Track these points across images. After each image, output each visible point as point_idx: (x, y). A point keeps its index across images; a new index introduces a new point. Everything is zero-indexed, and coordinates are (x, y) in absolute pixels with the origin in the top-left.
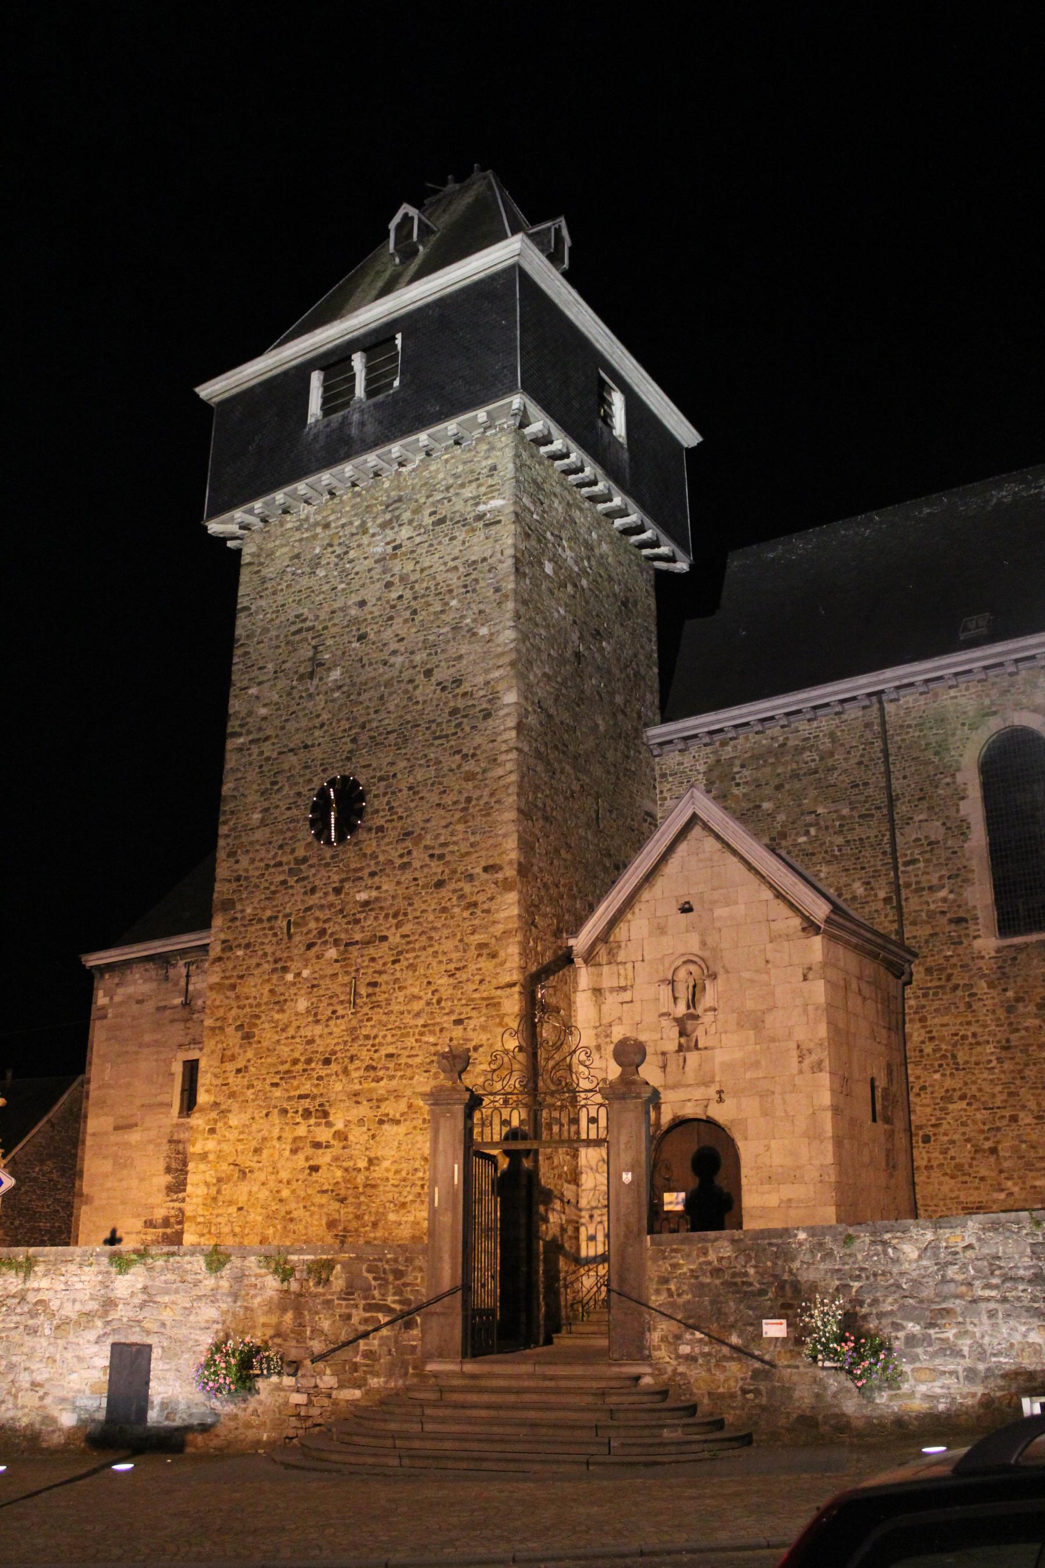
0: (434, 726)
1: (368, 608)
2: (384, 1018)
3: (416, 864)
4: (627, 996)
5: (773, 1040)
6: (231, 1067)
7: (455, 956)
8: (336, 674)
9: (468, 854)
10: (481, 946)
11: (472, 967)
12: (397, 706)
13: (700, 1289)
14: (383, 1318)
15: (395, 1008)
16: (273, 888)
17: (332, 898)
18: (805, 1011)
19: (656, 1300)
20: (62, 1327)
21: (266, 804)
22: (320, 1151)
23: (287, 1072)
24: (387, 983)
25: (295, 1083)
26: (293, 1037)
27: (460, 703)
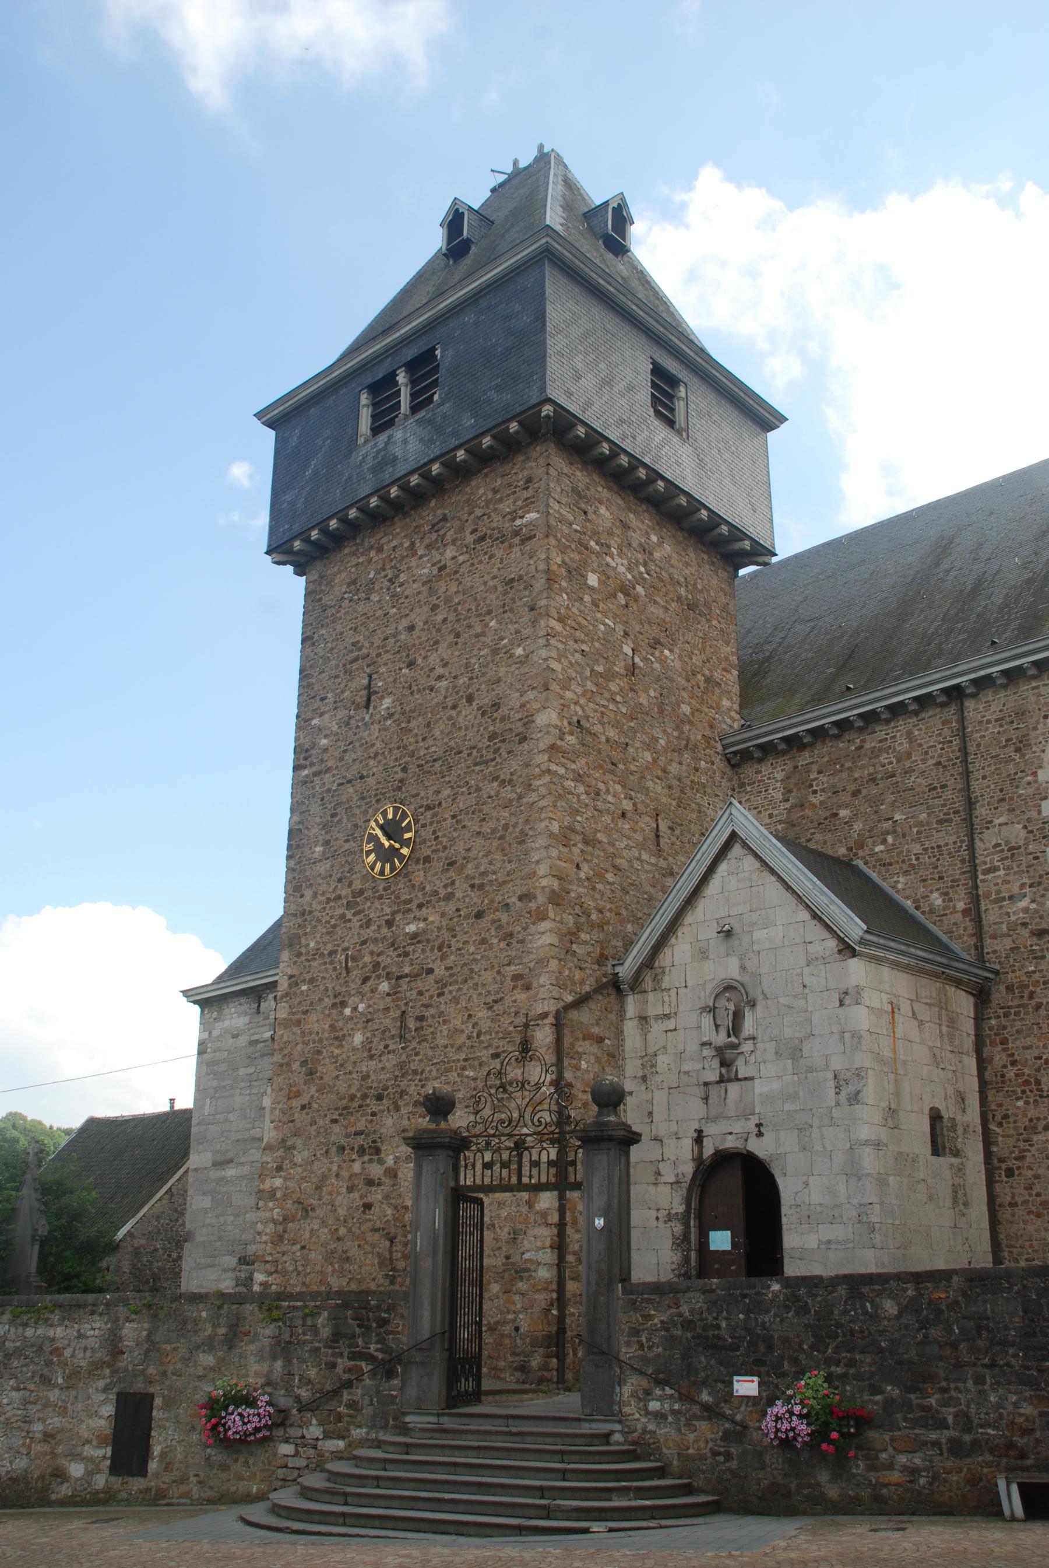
0: (474, 752)
1: (416, 633)
2: (430, 1053)
3: (459, 894)
4: (670, 1024)
5: (810, 1070)
6: (296, 1103)
7: (492, 988)
8: (387, 702)
9: (505, 882)
10: (517, 977)
11: (508, 1000)
12: (442, 732)
13: (671, 1341)
14: (365, 1366)
15: (440, 1042)
16: (333, 922)
17: (384, 930)
18: (842, 1038)
19: (627, 1352)
20: (74, 1377)
21: (328, 837)
22: (374, 1189)
23: (345, 1108)
24: (433, 1016)
25: (352, 1119)
26: (350, 1073)
27: (498, 727)
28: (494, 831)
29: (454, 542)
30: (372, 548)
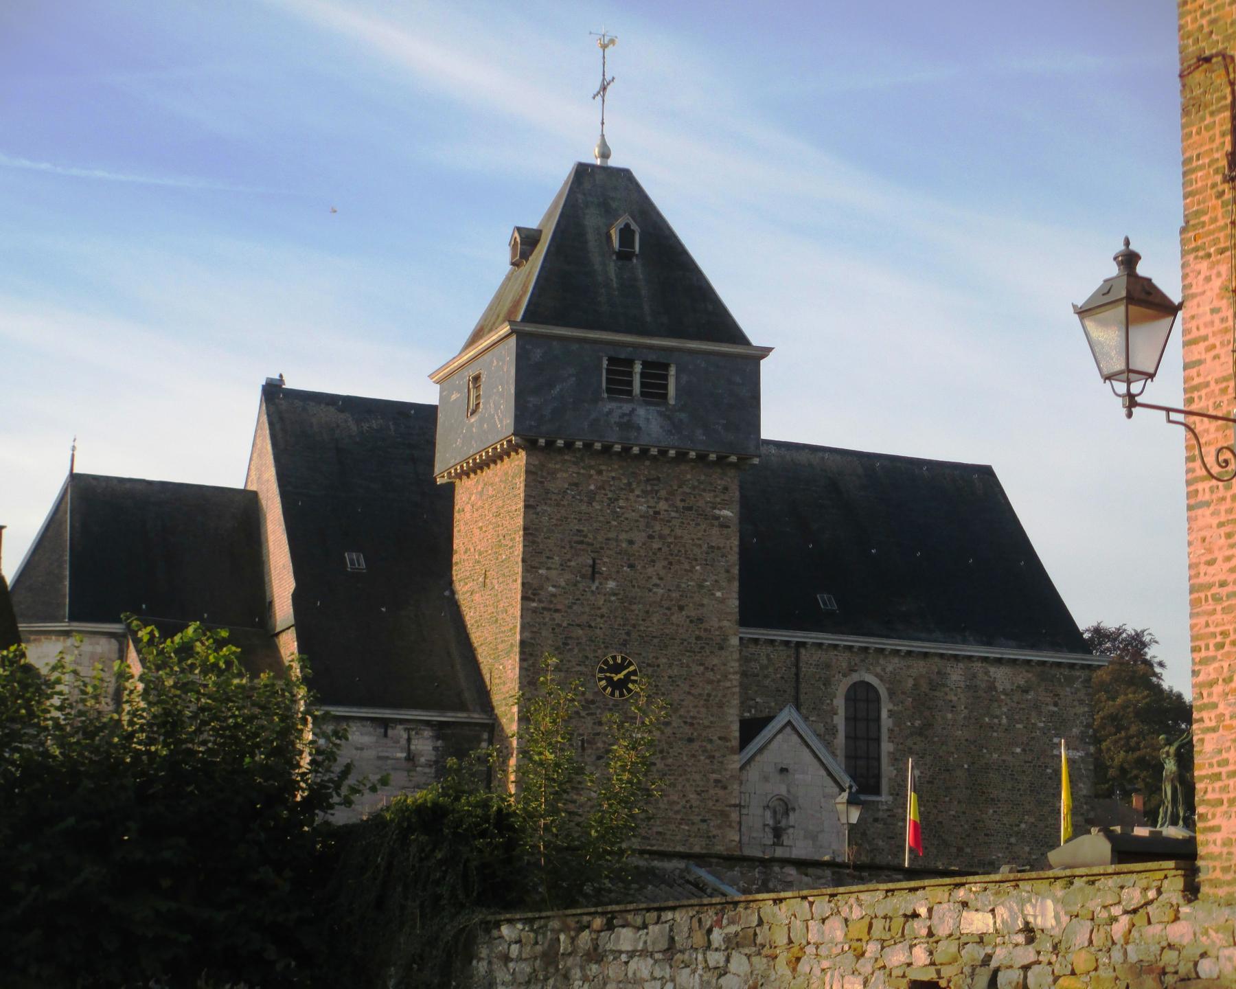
1: (635, 547)
3: (674, 724)
7: (701, 783)
8: (611, 584)
9: (709, 727)
10: (717, 781)
11: (712, 792)
27: (703, 634)
28: (700, 695)
29: (666, 500)
30: (591, 467)
